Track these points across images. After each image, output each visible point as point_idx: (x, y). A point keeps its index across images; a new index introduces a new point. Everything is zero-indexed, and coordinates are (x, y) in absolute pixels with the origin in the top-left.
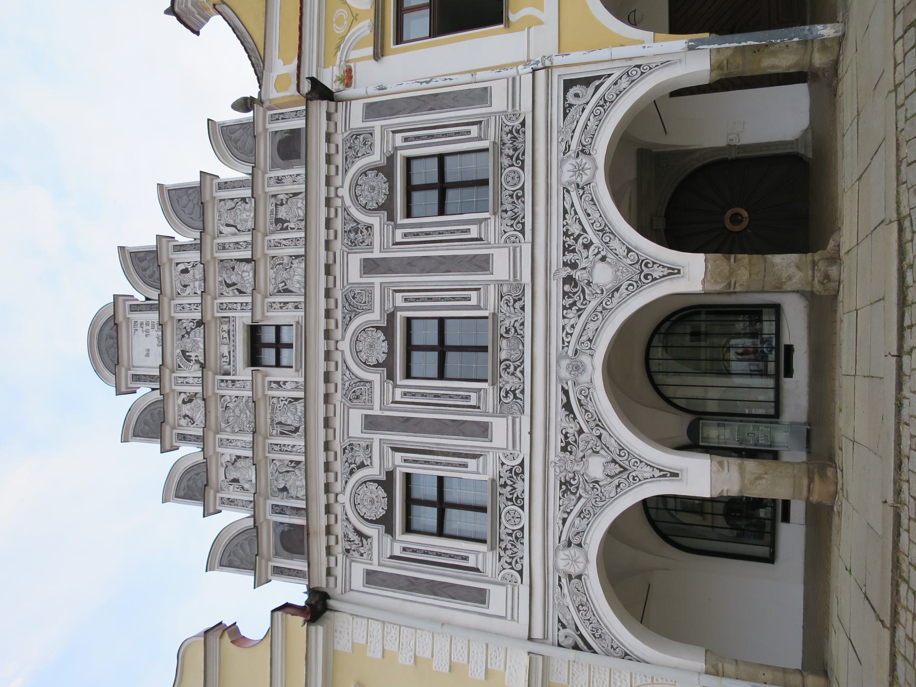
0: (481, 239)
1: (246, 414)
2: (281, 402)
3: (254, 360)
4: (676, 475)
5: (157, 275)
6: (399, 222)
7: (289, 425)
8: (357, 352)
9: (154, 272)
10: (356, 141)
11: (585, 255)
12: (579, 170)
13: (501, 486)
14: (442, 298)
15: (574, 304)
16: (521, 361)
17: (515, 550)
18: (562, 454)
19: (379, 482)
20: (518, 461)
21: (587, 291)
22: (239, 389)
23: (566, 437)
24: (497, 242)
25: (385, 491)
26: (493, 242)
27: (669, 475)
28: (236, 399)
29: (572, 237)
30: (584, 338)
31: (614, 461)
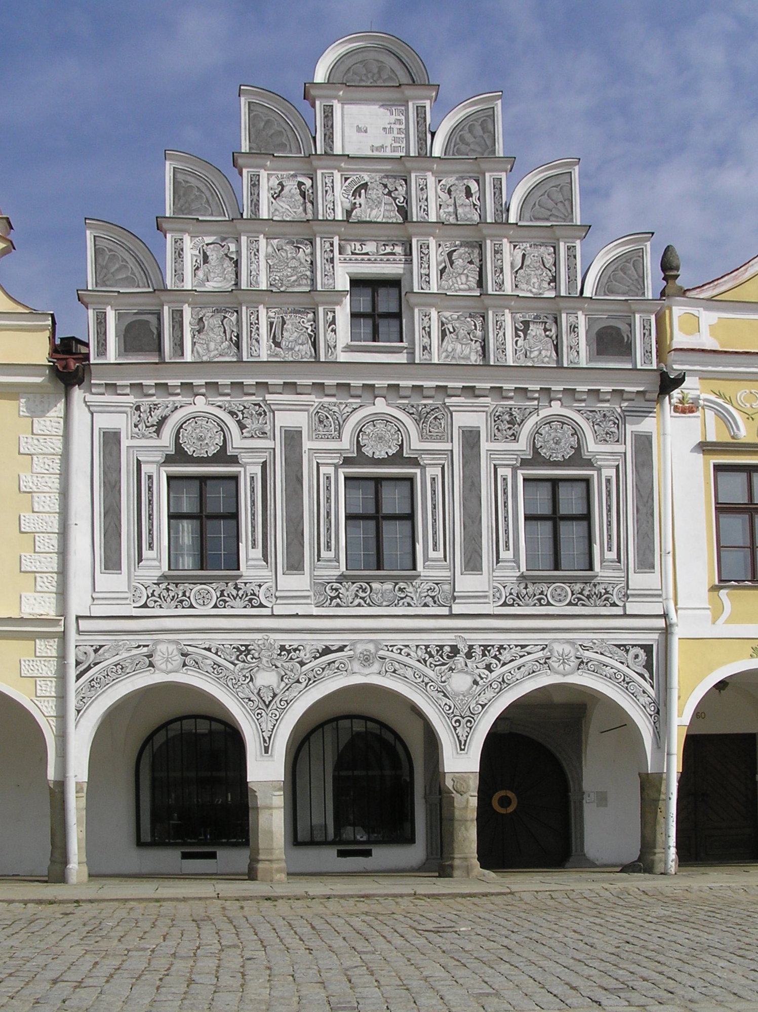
0: (498, 562)
1: (292, 276)
2: (310, 324)
3: (357, 283)
4: (266, 752)
5: (463, 147)
6: (520, 472)
7: (282, 334)
8: (373, 421)
9: (468, 144)
10: (611, 423)
11: (479, 665)
12: (564, 660)
13: (236, 584)
14: (435, 520)
15: (431, 656)
16: (371, 604)
17: (169, 600)
18: (277, 646)
19: (224, 447)
20: (265, 603)
21: (443, 668)
22: (324, 270)
23: (295, 650)
24: (494, 578)
25: (214, 454)
26: (495, 574)
27: (266, 745)
28: (309, 262)
29: (497, 653)
30: (397, 666)
31: (275, 695)
